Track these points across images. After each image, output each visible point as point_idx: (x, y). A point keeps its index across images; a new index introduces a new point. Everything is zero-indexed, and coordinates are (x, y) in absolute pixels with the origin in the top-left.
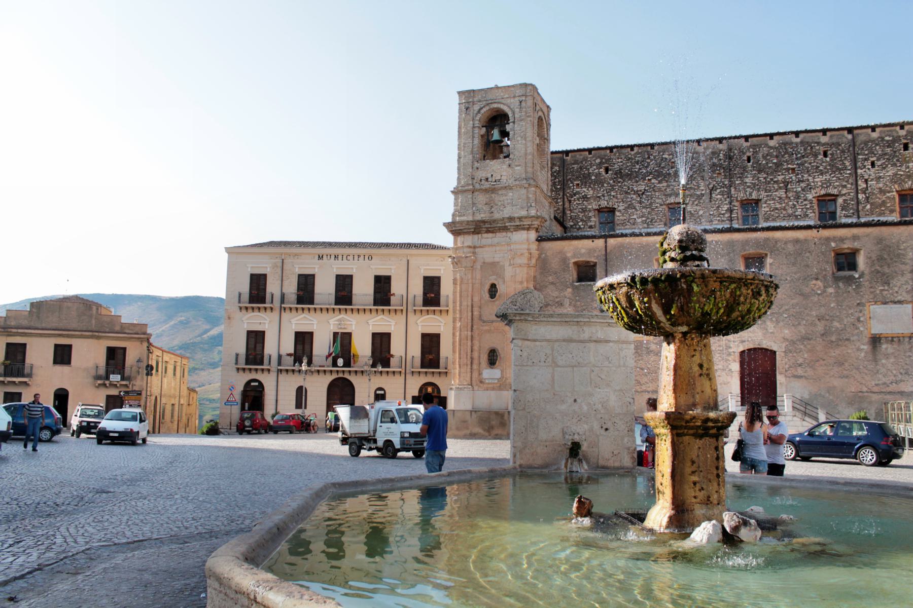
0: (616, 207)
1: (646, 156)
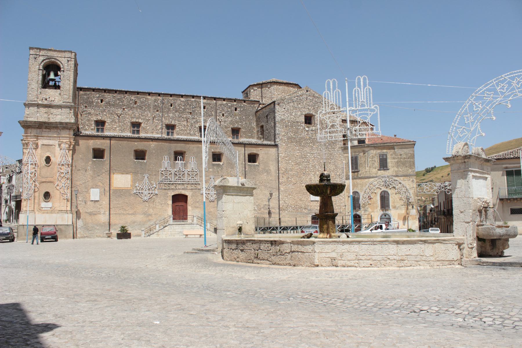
0: (106, 120)
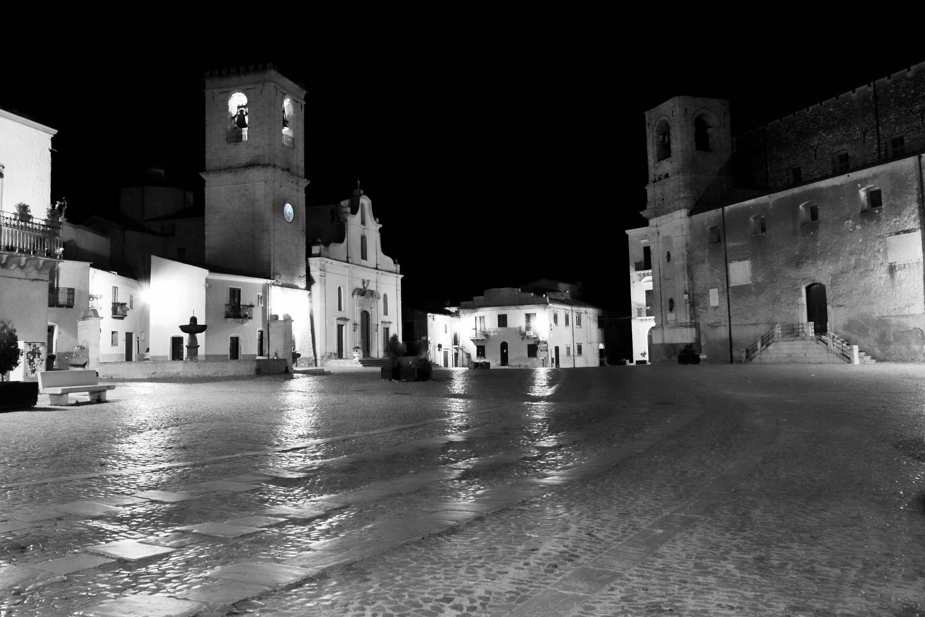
1: (818, 113)
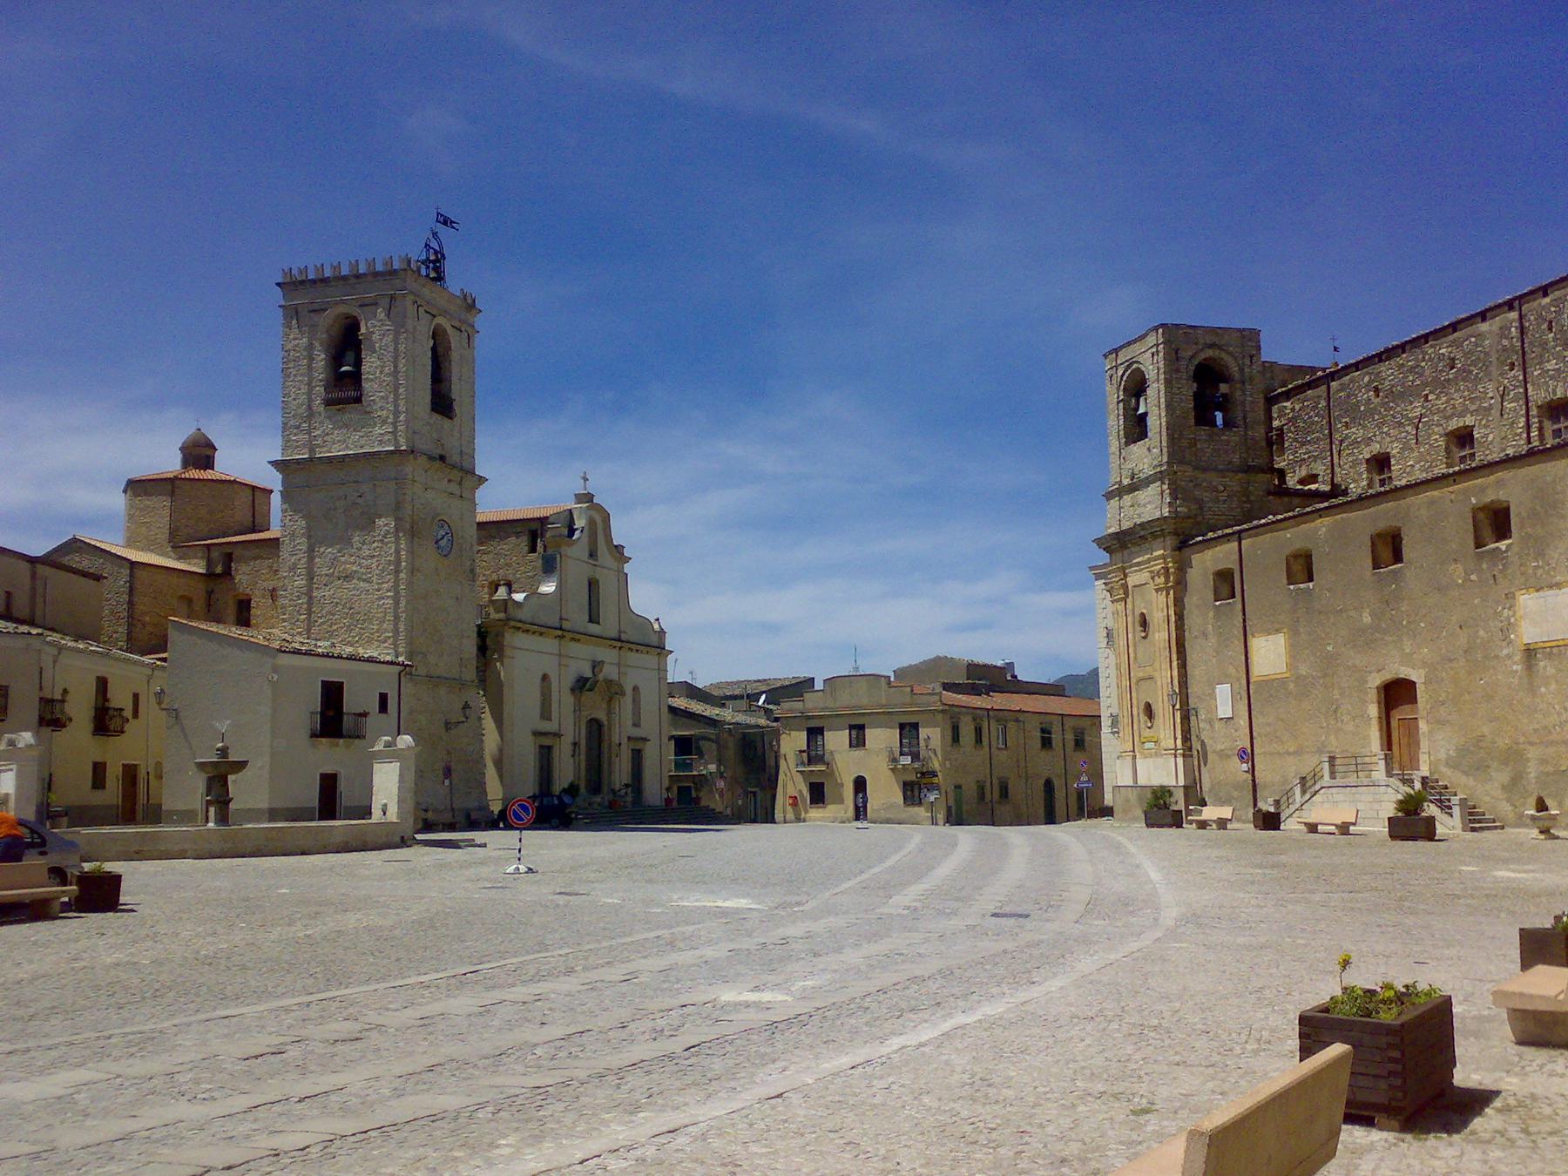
0: (1388, 450)
